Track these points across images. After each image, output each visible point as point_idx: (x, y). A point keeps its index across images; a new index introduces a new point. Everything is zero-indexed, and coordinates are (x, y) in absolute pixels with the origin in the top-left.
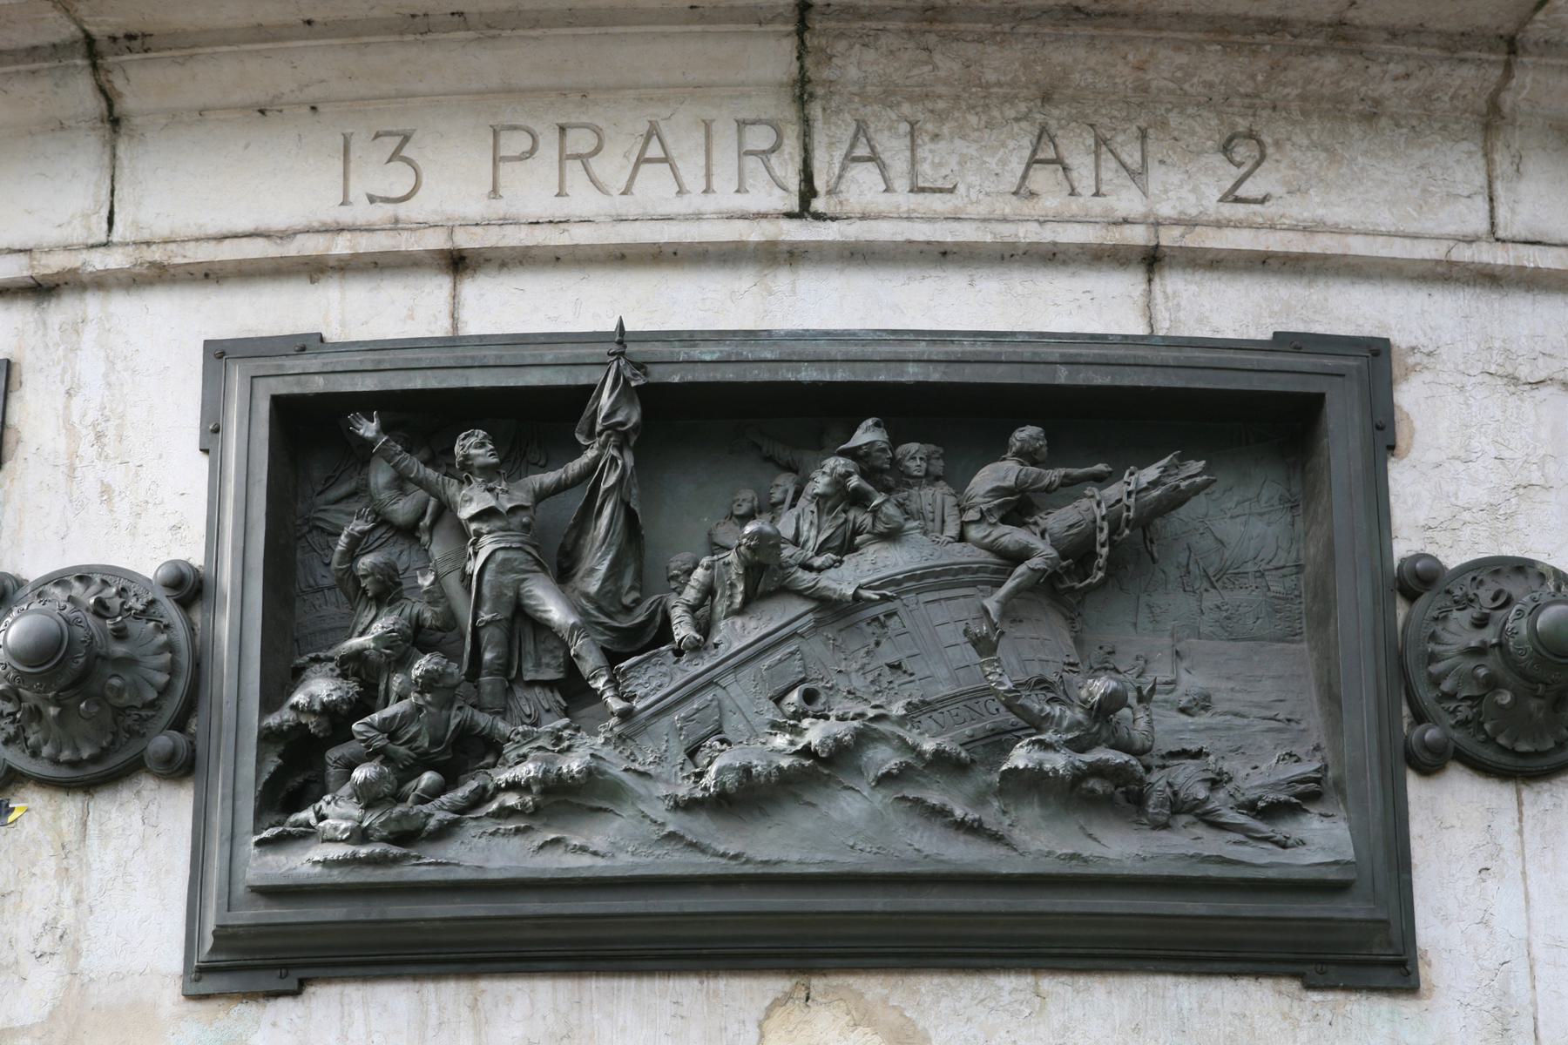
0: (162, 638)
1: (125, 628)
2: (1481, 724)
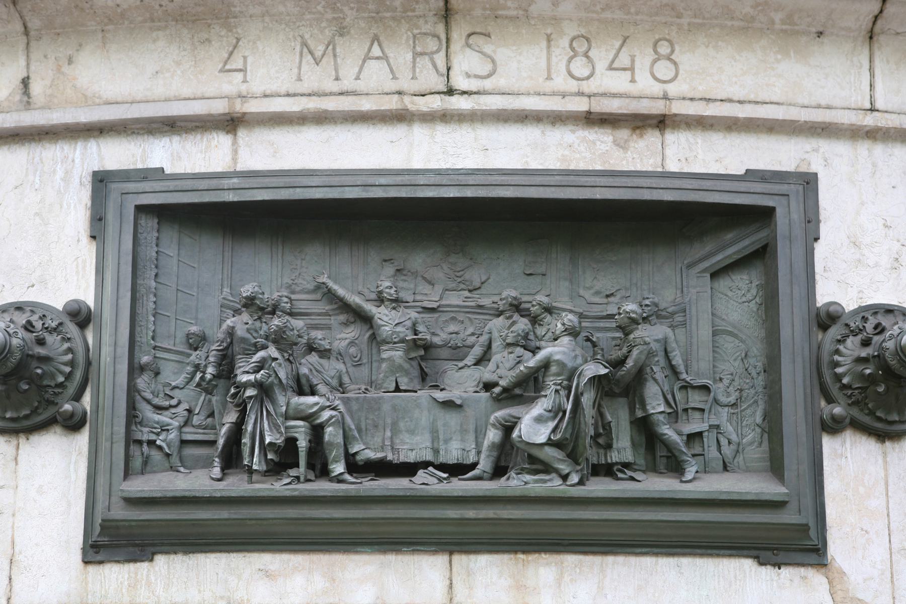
0: (66, 345)
1: (44, 339)
2: (866, 404)
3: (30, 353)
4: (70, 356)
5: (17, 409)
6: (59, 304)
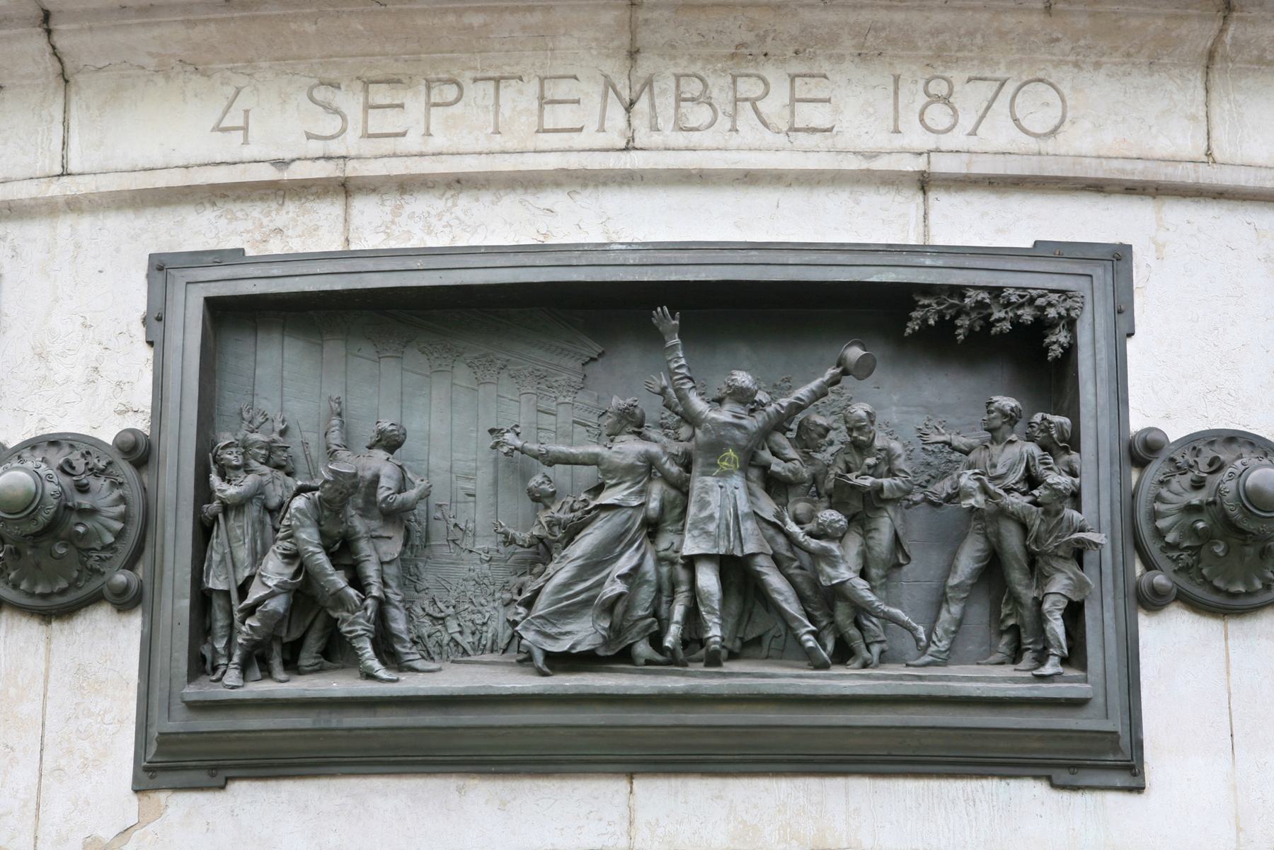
0: (117, 493)
3: (70, 504)
4: (122, 508)
5: (51, 580)
6: (108, 436)
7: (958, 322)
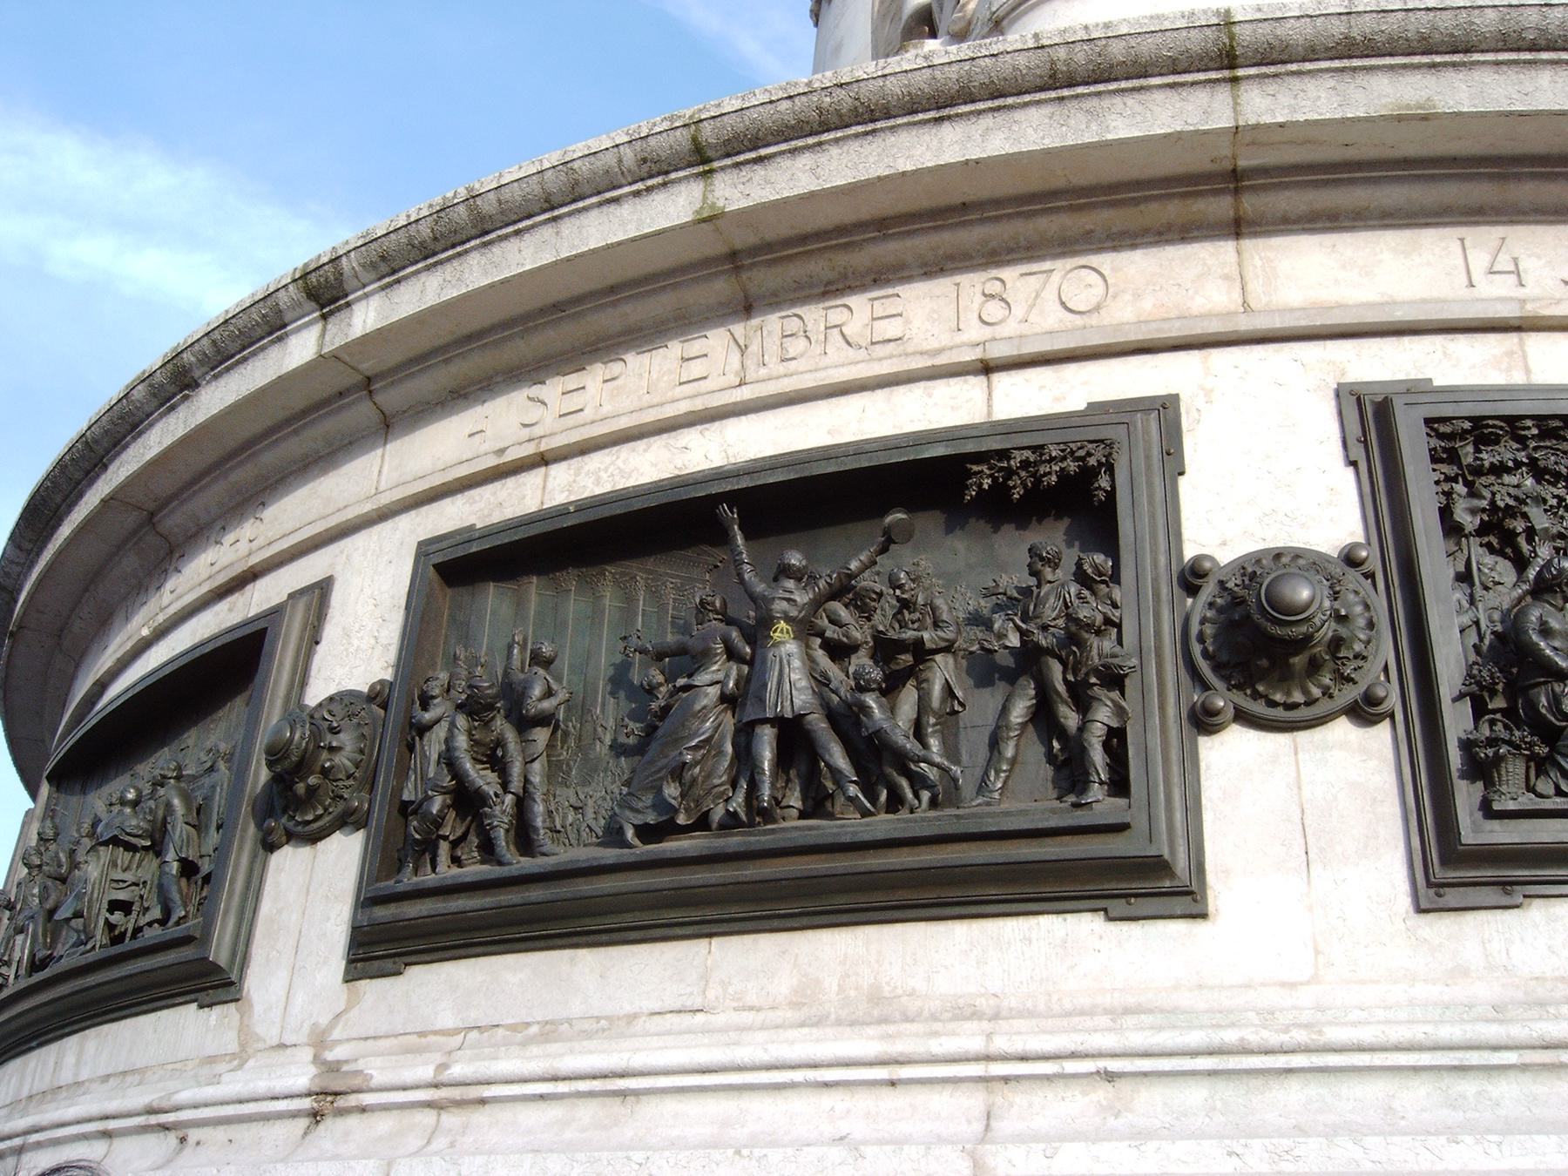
7: (1011, 483)
